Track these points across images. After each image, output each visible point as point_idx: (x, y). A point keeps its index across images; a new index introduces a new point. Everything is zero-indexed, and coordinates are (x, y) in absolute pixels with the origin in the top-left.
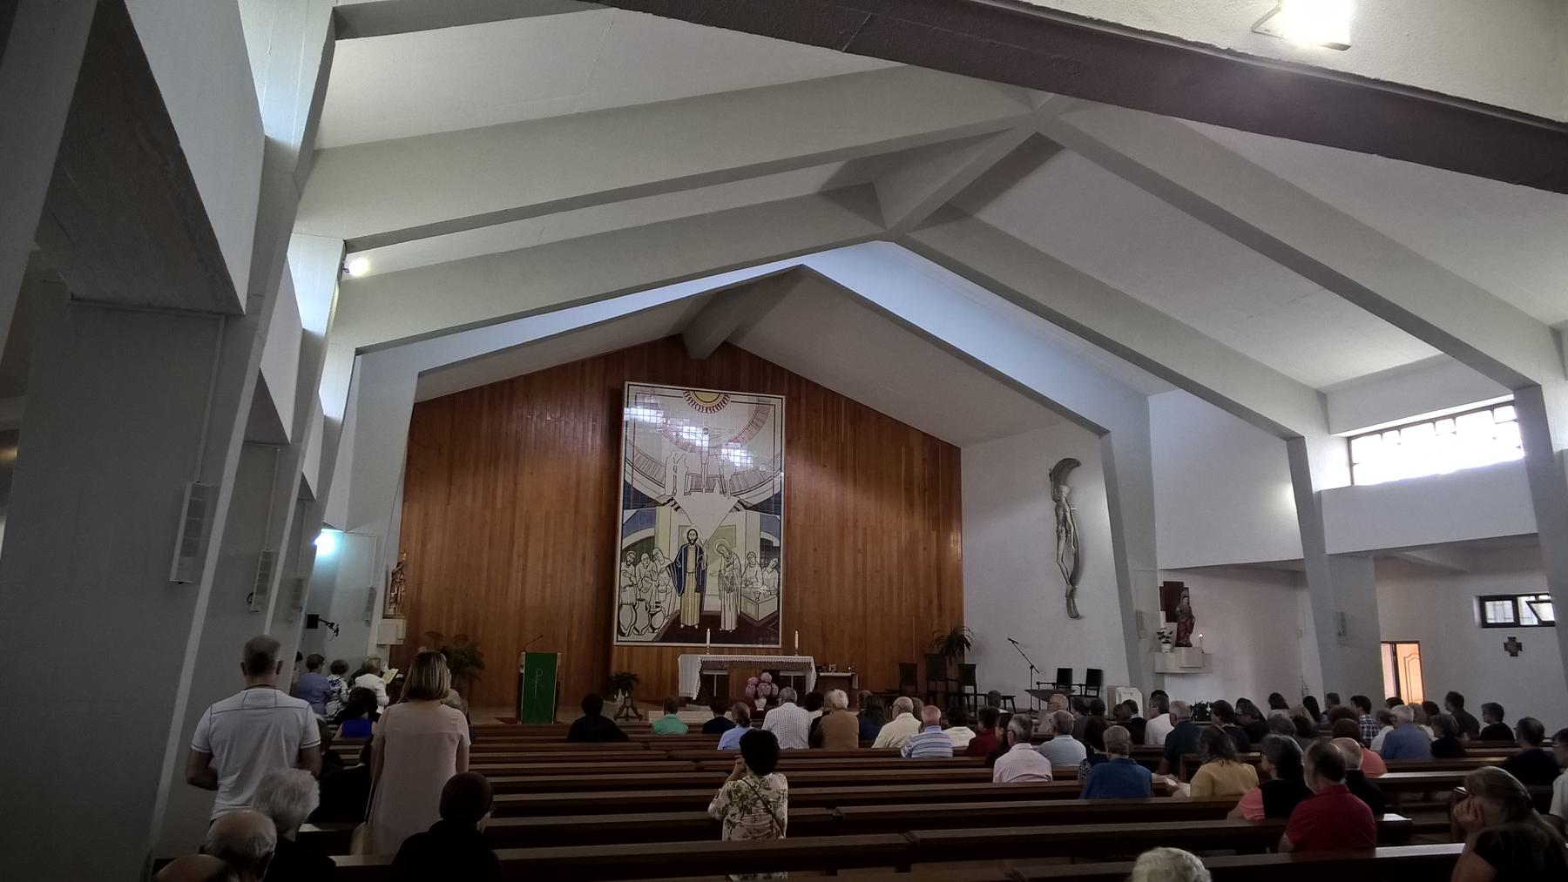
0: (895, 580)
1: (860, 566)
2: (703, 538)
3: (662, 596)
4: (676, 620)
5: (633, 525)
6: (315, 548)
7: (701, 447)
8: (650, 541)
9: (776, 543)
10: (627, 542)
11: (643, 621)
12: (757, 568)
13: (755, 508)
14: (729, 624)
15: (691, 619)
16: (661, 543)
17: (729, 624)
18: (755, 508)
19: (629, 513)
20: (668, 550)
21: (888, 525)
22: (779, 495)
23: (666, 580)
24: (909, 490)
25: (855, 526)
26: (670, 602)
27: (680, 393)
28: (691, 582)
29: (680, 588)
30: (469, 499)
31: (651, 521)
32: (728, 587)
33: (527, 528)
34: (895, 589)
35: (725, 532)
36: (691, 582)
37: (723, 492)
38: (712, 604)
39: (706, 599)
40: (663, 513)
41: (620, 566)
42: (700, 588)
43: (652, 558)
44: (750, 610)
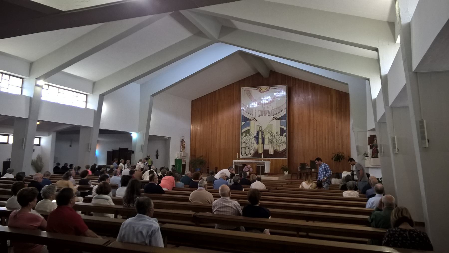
0: (327, 138)
1: (315, 134)
2: (263, 129)
3: (252, 145)
4: (256, 152)
5: (244, 126)
6: (132, 137)
7: (264, 103)
8: (249, 130)
9: (285, 129)
10: (243, 131)
11: (248, 152)
12: (280, 136)
13: (279, 119)
14: (271, 152)
15: (261, 151)
16: (252, 130)
17: (271, 152)
18: (279, 119)
19: (243, 123)
20: (254, 132)
21: (326, 120)
22: (285, 115)
23: (253, 141)
24: (331, 108)
25: (314, 122)
26: (255, 147)
27: (256, 89)
28: (260, 141)
29: (257, 143)
30: (206, 122)
31: (249, 125)
32: (271, 141)
33: (220, 129)
34: (327, 141)
35: (270, 127)
36: (260, 141)
37: (269, 115)
38: (266, 147)
39: (265, 145)
40: (252, 122)
41: (241, 137)
42: (263, 143)
43: (250, 135)
44: (278, 148)
